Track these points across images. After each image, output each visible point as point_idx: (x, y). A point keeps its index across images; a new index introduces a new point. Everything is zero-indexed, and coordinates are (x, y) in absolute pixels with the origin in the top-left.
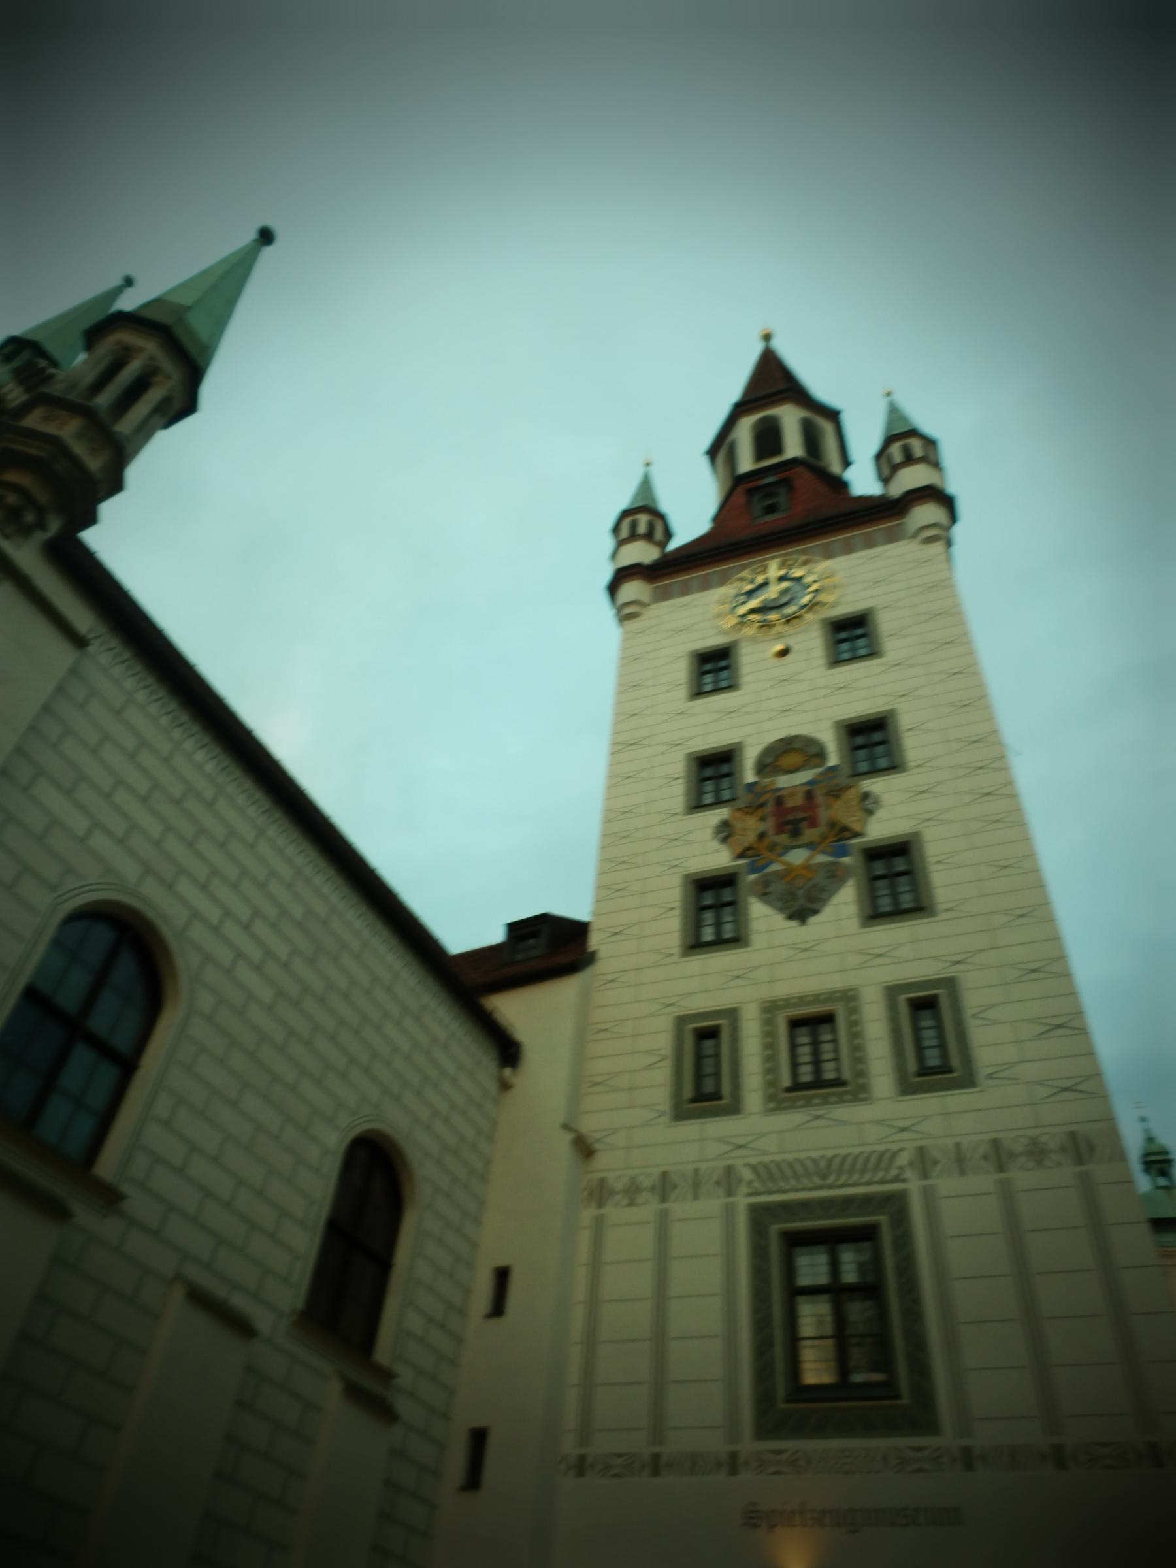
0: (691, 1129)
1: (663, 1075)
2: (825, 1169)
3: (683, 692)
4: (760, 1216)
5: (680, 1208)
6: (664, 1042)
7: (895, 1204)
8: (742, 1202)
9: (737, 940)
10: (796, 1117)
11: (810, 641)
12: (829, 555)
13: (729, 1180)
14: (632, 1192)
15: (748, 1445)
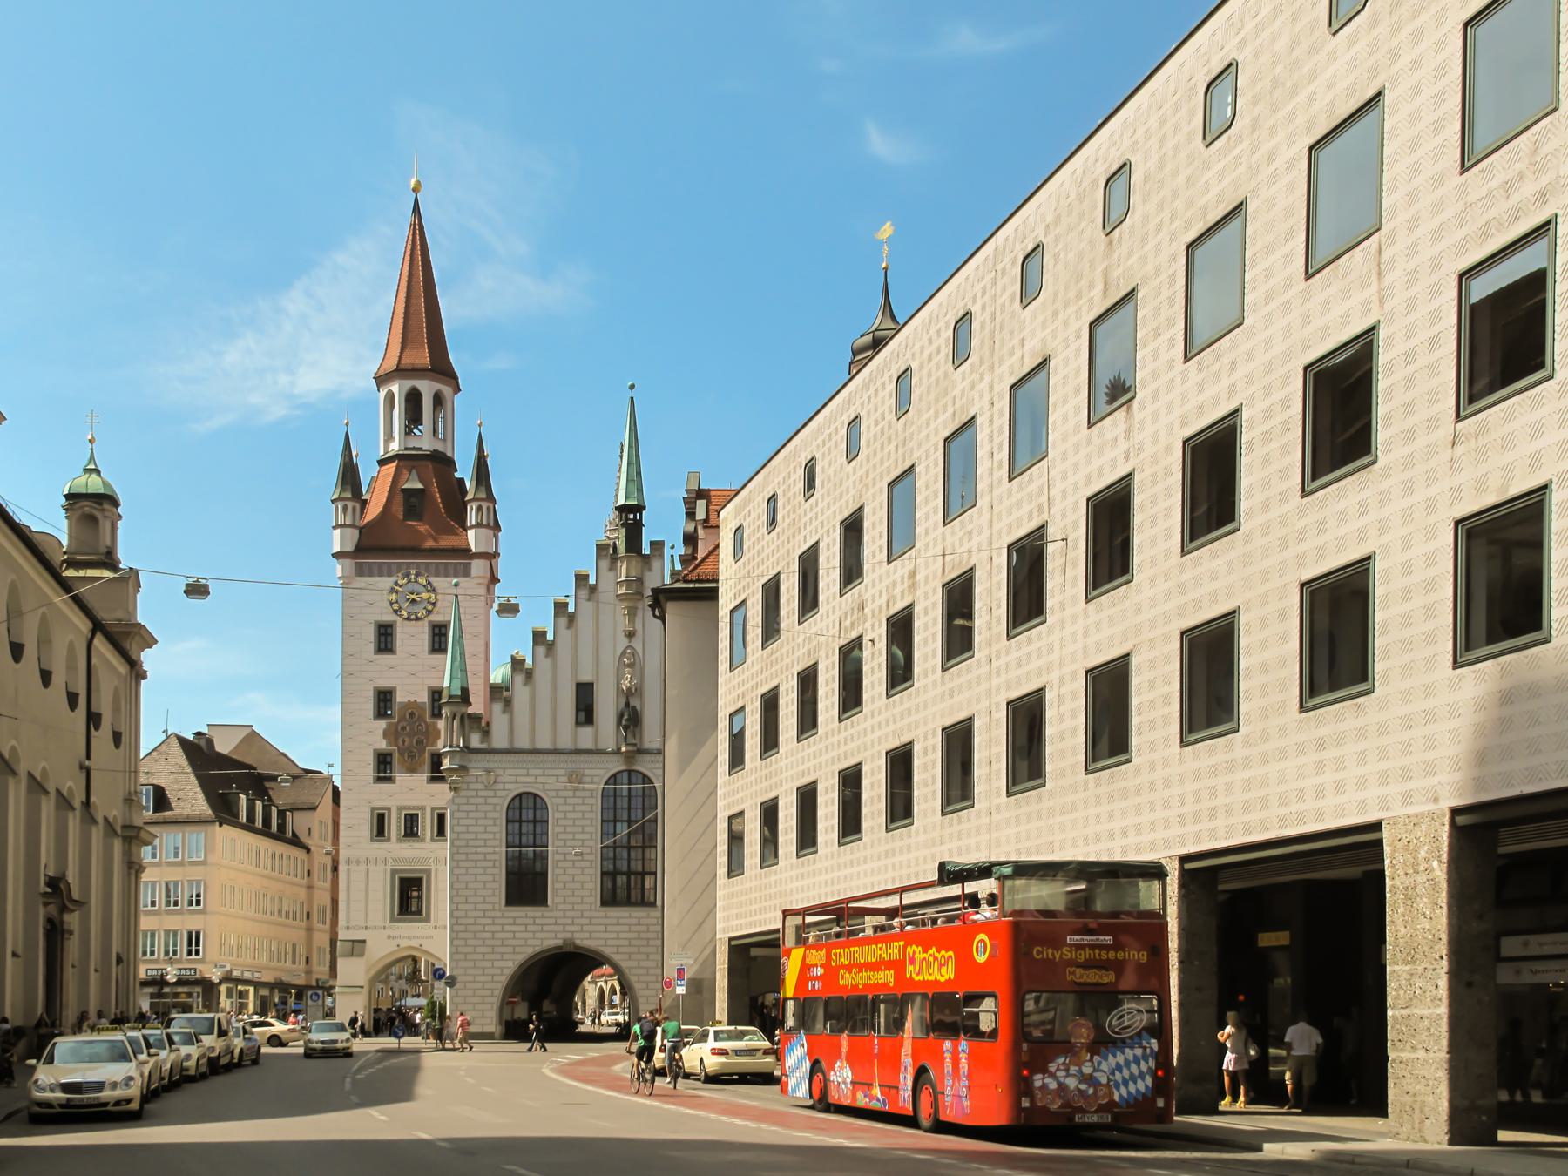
0: (376, 845)
1: (367, 827)
2: (411, 861)
3: (372, 647)
4: (394, 872)
5: (372, 867)
6: (368, 816)
7: (428, 872)
8: (389, 867)
9: (390, 780)
10: (404, 845)
11: (422, 632)
12: (437, 575)
13: (385, 862)
14: (358, 862)
15: (388, 924)
